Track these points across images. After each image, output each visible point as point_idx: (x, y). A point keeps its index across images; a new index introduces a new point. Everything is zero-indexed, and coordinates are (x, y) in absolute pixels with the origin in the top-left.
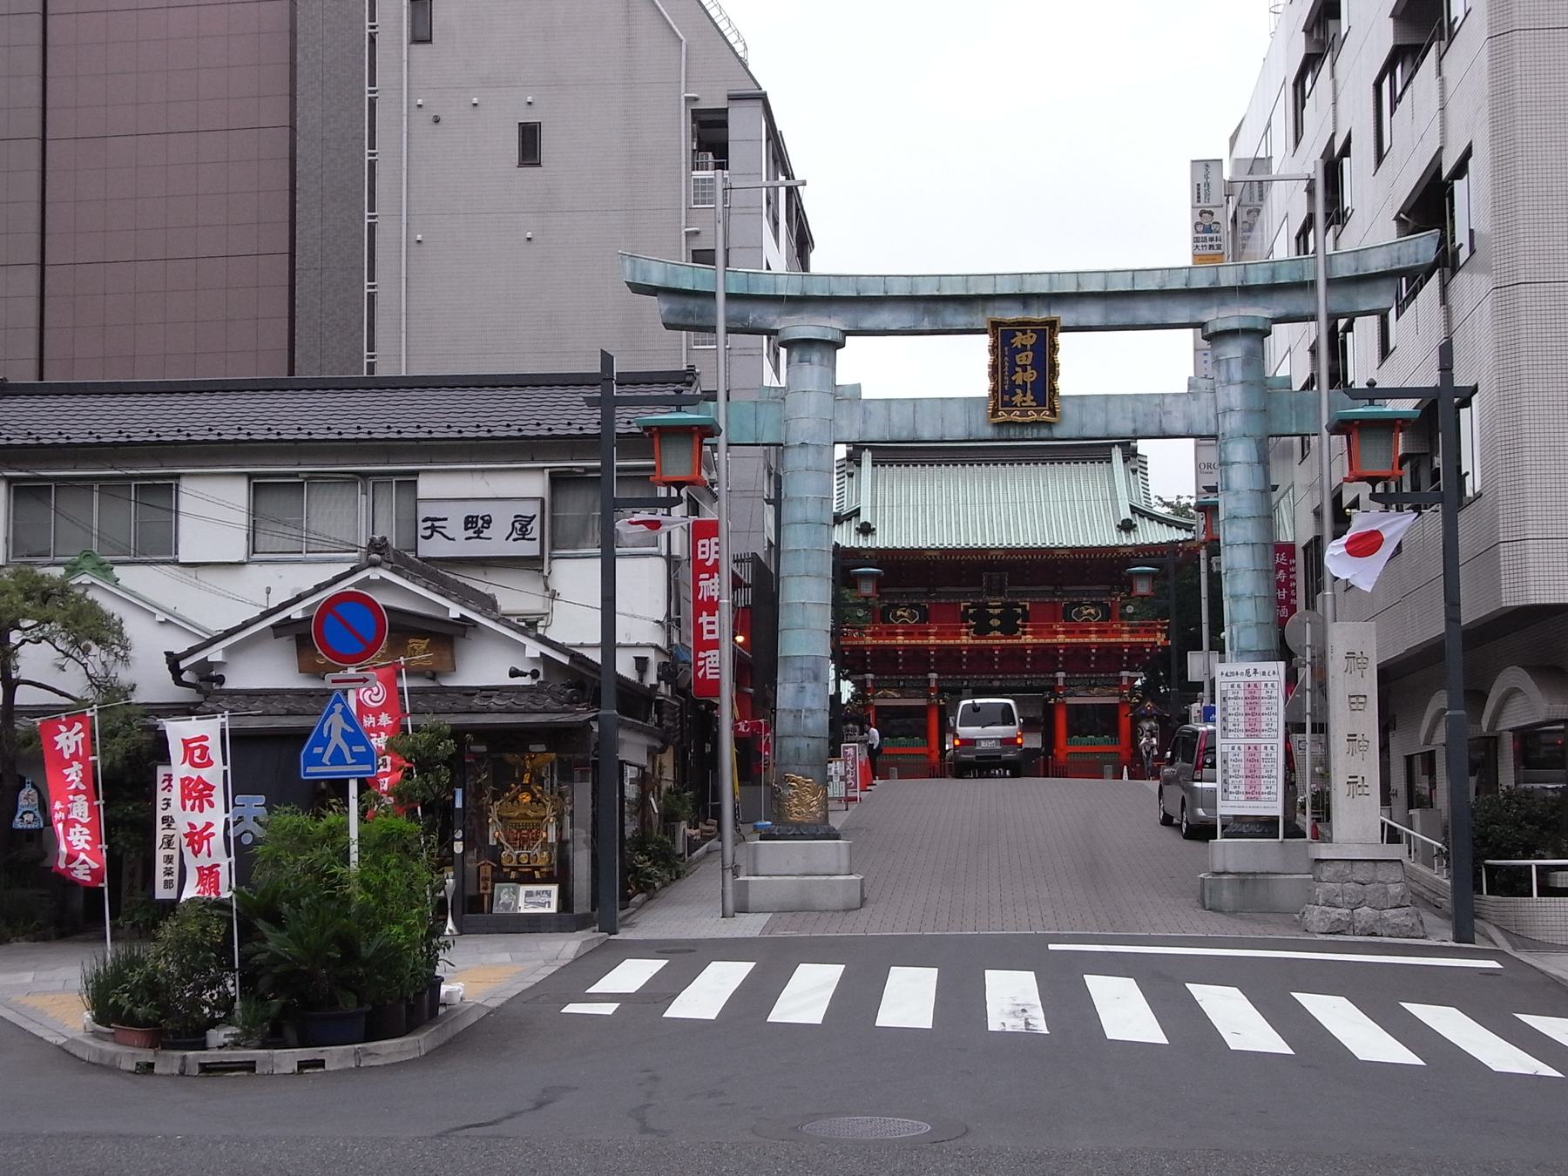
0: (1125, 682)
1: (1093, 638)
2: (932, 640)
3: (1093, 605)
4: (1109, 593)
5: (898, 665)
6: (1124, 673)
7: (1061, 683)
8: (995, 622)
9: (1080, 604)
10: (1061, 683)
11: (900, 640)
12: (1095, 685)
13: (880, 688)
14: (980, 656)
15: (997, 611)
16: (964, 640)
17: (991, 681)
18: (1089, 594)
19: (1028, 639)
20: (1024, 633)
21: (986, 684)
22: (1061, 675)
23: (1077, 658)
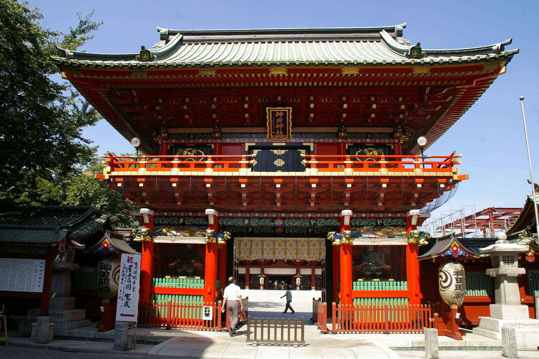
0: (414, 222)
1: (383, 172)
2: (209, 172)
3: (377, 146)
4: (391, 136)
5: (174, 200)
6: (413, 212)
7: (347, 222)
8: (279, 163)
9: (363, 146)
10: (347, 222)
11: (175, 172)
12: (382, 226)
13: (159, 224)
14: (261, 190)
15: (283, 152)
16: (245, 172)
17: (273, 219)
18: (372, 135)
19: (312, 172)
20: (309, 166)
21: (268, 223)
22: (347, 213)
23: (364, 194)
